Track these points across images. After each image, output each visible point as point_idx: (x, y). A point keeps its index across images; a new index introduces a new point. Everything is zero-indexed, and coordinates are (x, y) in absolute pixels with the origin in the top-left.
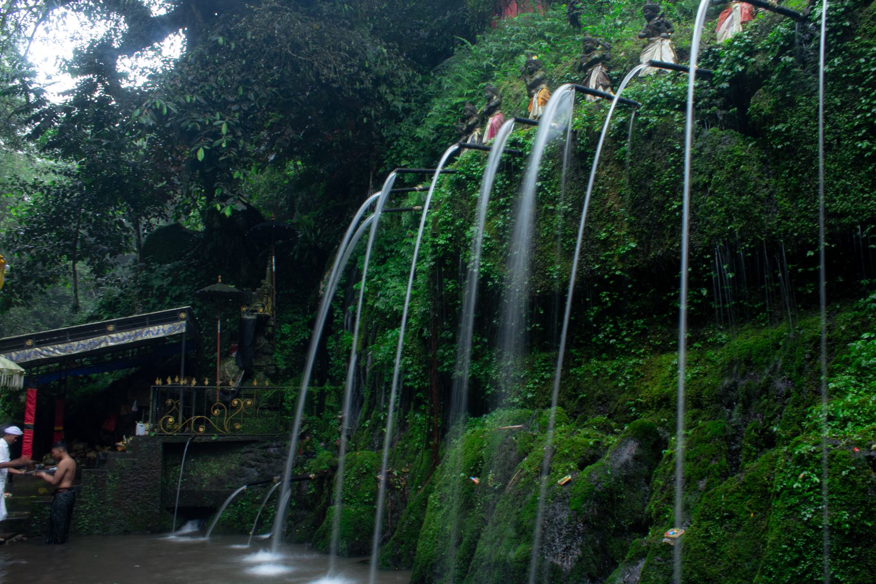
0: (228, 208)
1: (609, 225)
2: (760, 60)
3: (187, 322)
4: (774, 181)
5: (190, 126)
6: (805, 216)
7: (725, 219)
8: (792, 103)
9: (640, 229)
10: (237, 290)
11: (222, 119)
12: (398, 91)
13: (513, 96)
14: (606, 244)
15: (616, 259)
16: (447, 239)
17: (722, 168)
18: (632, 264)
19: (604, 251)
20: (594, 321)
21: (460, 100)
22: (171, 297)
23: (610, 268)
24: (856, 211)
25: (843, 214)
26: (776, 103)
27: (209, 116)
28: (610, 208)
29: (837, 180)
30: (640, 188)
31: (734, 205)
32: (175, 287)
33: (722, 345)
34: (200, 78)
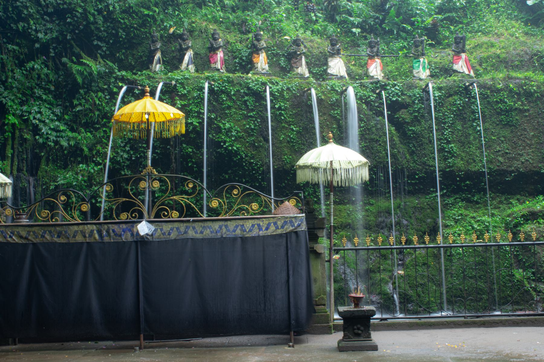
8: (419, 121)
16: (198, 123)
33: (372, 205)
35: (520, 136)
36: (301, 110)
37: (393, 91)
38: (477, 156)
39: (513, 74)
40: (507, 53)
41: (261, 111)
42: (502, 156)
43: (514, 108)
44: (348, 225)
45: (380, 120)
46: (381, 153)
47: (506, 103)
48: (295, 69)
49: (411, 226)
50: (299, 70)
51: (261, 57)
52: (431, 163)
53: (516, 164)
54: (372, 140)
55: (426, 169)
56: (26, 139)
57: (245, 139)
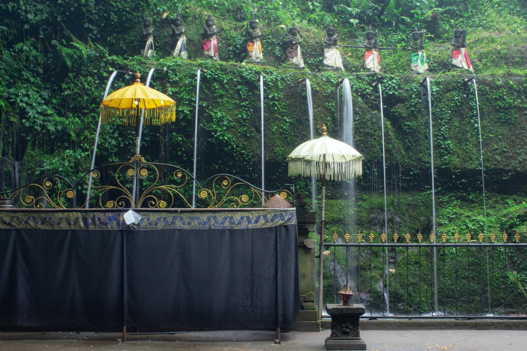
8: (415, 116)
16: (188, 111)
33: (365, 200)
35: (518, 135)
36: (295, 102)
37: (390, 85)
38: (474, 154)
39: (514, 71)
40: (508, 49)
41: (253, 101)
42: (500, 154)
43: (513, 105)
44: (339, 221)
45: (375, 114)
46: (376, 148)
47: (505, 100)
48: (290, 59)
49: (404, 224)
50: (295, 60)
51: (255, 45)
52: (427, 160)
53: (514, 163)
54: (367, 134)
55: (421, 165)
56: (12, 122)
57: (236, 130)
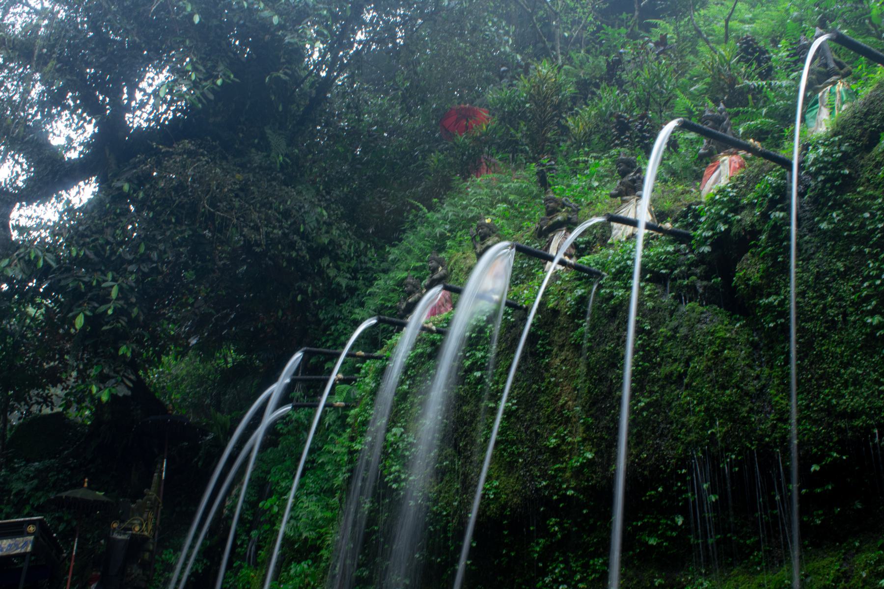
0: (107, 391)
1: (561, 429)
2: (747, 218)
3: (36, 539)
4: (767, 371)
5: (71, 285)
6: (808, 417)
7: (705, 421)
9: (599, 435)
10: (105, 499)
11: (114, 280)
12: (344, 266)
13: (465, 270)
14: (556, 453)
15: (568, 474)
17: (701, 354)
18: (588, 481)
19: (554, 463)
20: (540, 559)
21: (405, 274)
22: (33, 506)
23: (560, 486)
24: (871, 409)
25: (854, 414)
26: (766, 270)
27: (98, 276)
28: (563, 406)
29: (845, 368)
30: (601, 380)
31: (716, 402)
32: (39, 494)
34: (94, 229)
55: (840, 431)
